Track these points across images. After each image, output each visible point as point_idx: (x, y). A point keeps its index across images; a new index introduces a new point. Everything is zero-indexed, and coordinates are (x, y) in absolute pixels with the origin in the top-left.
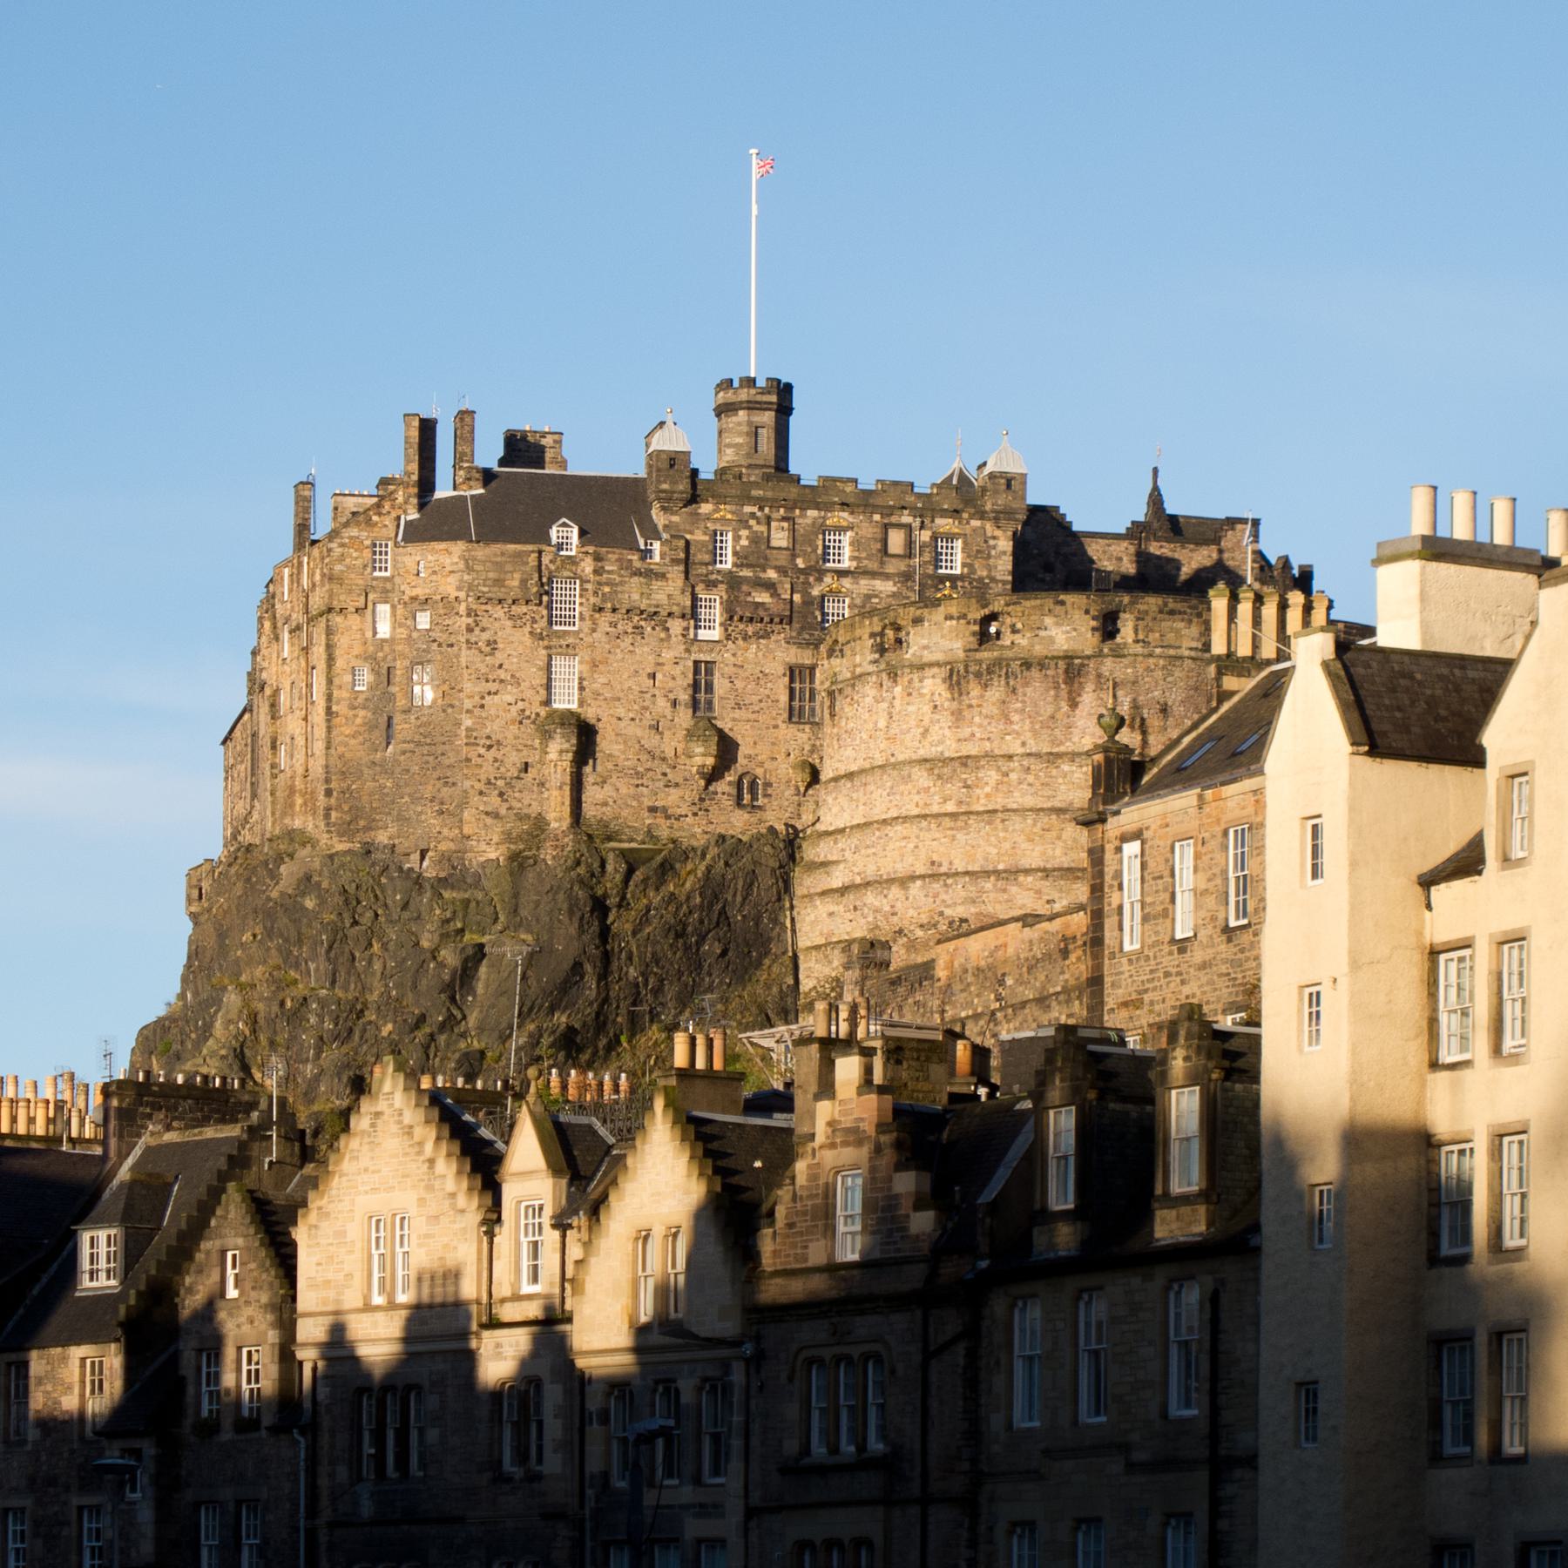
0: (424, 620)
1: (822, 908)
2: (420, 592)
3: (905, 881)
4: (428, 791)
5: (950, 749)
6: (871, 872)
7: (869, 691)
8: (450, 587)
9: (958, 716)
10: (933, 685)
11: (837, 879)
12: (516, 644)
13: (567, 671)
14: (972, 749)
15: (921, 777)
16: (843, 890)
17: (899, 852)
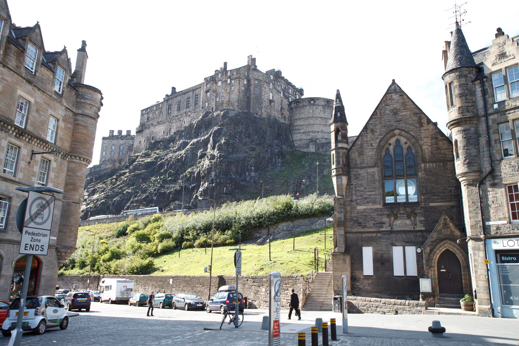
0: (256, 82)
1: (299, 135)
2: (257, 78)
3: (318, 132)
4: (257, 105)
5: (323, 116)
6: (311, 130)
7: (308, 108)
8: (261, 78)
9: (324, 112)
10: (320, 108)
11: (302, 131)
12: (267, 88)
13: (271, 94)
14: (326, 117)
15: (320, 120)
16: (304, 133)
17: (316, 128)
